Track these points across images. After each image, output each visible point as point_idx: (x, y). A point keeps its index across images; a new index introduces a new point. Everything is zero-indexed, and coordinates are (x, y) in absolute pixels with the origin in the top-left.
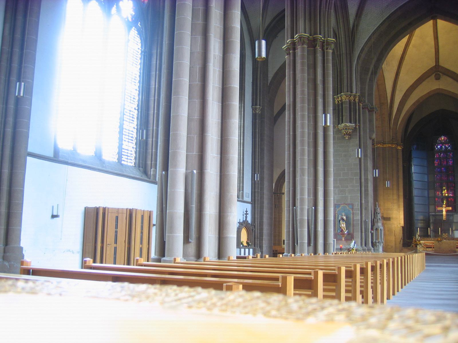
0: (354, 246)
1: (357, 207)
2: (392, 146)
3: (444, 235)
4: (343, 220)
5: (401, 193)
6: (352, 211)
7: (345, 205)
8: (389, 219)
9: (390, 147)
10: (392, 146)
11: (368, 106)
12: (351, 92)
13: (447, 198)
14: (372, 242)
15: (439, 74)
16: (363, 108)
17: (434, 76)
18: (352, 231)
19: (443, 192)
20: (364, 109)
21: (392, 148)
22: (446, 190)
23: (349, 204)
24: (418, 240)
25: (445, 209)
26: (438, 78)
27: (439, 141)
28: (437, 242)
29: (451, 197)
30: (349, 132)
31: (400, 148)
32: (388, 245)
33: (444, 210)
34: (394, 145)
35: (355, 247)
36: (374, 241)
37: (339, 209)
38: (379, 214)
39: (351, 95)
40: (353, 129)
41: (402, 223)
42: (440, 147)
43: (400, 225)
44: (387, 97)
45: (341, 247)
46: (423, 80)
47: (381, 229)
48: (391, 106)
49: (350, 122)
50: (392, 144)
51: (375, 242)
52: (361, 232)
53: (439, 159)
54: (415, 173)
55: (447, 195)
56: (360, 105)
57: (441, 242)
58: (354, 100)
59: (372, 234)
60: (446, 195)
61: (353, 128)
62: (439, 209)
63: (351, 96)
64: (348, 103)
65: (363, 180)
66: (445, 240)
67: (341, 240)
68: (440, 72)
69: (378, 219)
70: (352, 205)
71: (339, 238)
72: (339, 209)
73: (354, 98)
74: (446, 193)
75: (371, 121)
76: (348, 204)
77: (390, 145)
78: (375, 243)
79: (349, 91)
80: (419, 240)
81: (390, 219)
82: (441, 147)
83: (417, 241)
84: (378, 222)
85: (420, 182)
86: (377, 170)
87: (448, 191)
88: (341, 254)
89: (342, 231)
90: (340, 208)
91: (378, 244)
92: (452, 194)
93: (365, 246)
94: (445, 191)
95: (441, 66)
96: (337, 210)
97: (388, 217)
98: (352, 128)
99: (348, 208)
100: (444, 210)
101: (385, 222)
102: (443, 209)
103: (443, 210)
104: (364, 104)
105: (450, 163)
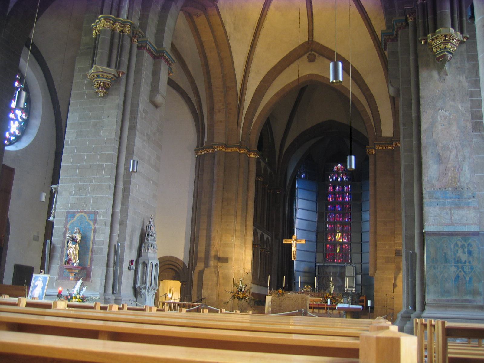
0: (81, 289)
1: (103, 218)
2: (240, 150)
3: (306, 288)
4: (74, 240)
6: (94, 224)
7: (83, 214)
8: (225, 260)
9: (237, 152)
10: (240, 150)
11: (147, 43)
12: (118, 15)
13: (342, 244)
15: (315, 56)
16: (139, 48)
17: (307, 55)
18: (89, 263)
19: (337, 237)
20: (141, 49)
21: (240, 154)
22: (340, 234)
23: (90, 213)
24: (241, 291)
26: (311, 60)
28: (277, 296)
30: (104, 83)
32: (221, 301)
34: (242, 150)
35: (82, 293)
36: (138, 284)
37: (72, 221)
38: (151, 235)
39: (116, 20)
40: (112, 78)
42: (335, 179)
43: (244, 270)
44: (235, 78)
45: (60, 293)
46: (291, 62)
48: (242, 93)
49: (109, 66)
50: (240, 147)
52: (108, 266)
53: (334, 193)
55: (341, 240)
56: (134, 41)
57: (283, 296)
58: (122, 31)
60: (340, 241)
61: (112, 76)
62: (286, 241)
63: (116, 22)
64: (109, 33)
65: (122, 171)
66: (289, 294)
67: (68, 278)
68: (316, 52)
69: (150, 245)
70: (96, 213)
71: (67, 276)
72: (72, 221)
73: (123, 27)
75: (156, 74)
76: (89, 213)
77: (237, 150)
78: (138, 290)
79: (113, 13)
80: (243, 290)
81: (228, 259)
82: (337, 178)
83: (240, 293)
84: (148, 251)
85: (304, 221)
87: (342, 236)
88: (119, 309)
89: (69, 261)
90: (75, 218)
91: (143, 291)
93: (113, 293)
94: (339, 235)
95: (316, 42)
96: (70, 222)
97: (225, 257)
98: (108, 75)
99: (87, 219)
101: (219, 264)
104: (140, 40)
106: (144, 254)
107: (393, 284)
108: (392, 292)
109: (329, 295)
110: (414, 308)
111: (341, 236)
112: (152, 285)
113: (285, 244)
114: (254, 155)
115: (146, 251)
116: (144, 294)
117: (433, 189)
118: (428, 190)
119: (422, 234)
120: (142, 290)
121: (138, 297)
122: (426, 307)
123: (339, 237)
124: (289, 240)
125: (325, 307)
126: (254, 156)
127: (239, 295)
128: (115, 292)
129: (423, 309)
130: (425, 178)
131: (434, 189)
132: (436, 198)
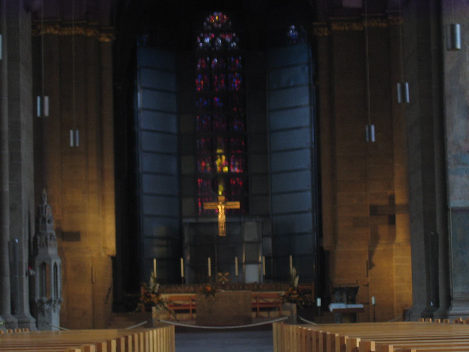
3: (221, 277)
5: (110, 165)
14: (32, 303)
19: (218, 162)
22: (224, 157)
24: (153, 293)
25: (223, 207)
27: (209, 24)
29: (236, 174)
31: (107, 40)
33: (221, 208)
36: (38, 298)
41: (111, 245)
47: (55, 266)
51: (41, 302)
54: (144, 109)
55: (226, 169)
57: (213, 295)
59: (31, 280)
62: (208, 206)
66: (223, 291)
69: (49, 237)
74: (225, 166)
77: (81, 31)
78: (38, 305)
80: (156, 291)
82: (213, 41)
84: (47, 245)
86: (46, 99)
87: (228, 160)
91: (47, 307)
92: (239, 167)
93: (13, 313)
94: (221, 158)
100: (221, 208)
101: (65, 244)
102: (219, 207)
103: (218, 209)
105: (236, 83)
106: (41, 251)
107: (367, 262)
108: (366, 275)
109: (292, 290)
110: (437, 305)
111: (226, 160)
112: (59, 297)
113: (207, 210)
114: (108, 37)
115: (43, 246)
116: (49, 311)
117: (459, 152)
118: (454, 153)
119: (445, 208)
120: (45, 305)
121: (40, 316)
122: (452, 302)
123: (220, 161)
124: (213, 204)
125: (258, 306)
126: (107, 40)
127: (152, 300)
128: (16, 312)
129: (448, 305)
130: (450, 138)
131: (461, 152)
132: (463, 164)
